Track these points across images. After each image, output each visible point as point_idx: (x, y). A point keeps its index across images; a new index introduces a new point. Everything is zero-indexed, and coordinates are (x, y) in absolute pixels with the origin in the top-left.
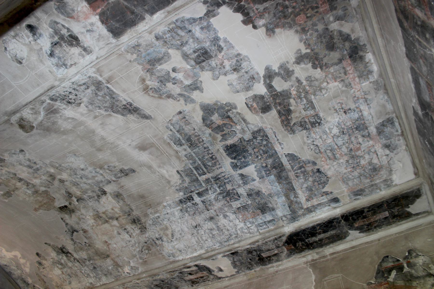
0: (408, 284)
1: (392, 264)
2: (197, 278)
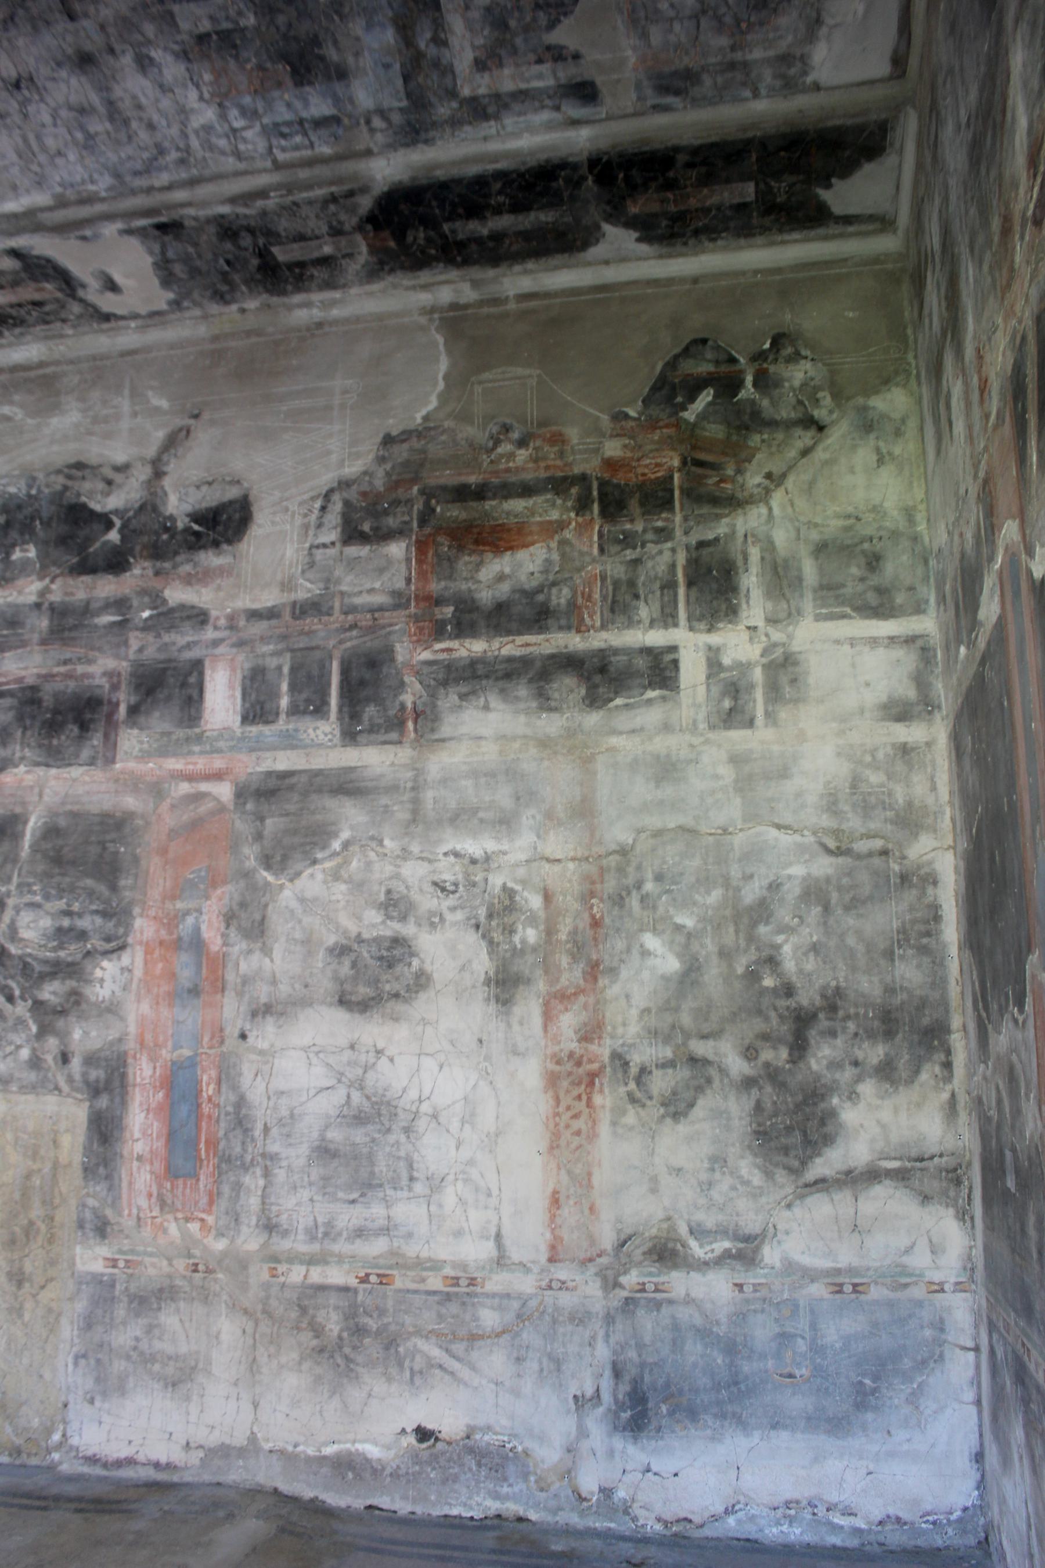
0: (734, 438)
1: (711, 368)
2: (20, 305)
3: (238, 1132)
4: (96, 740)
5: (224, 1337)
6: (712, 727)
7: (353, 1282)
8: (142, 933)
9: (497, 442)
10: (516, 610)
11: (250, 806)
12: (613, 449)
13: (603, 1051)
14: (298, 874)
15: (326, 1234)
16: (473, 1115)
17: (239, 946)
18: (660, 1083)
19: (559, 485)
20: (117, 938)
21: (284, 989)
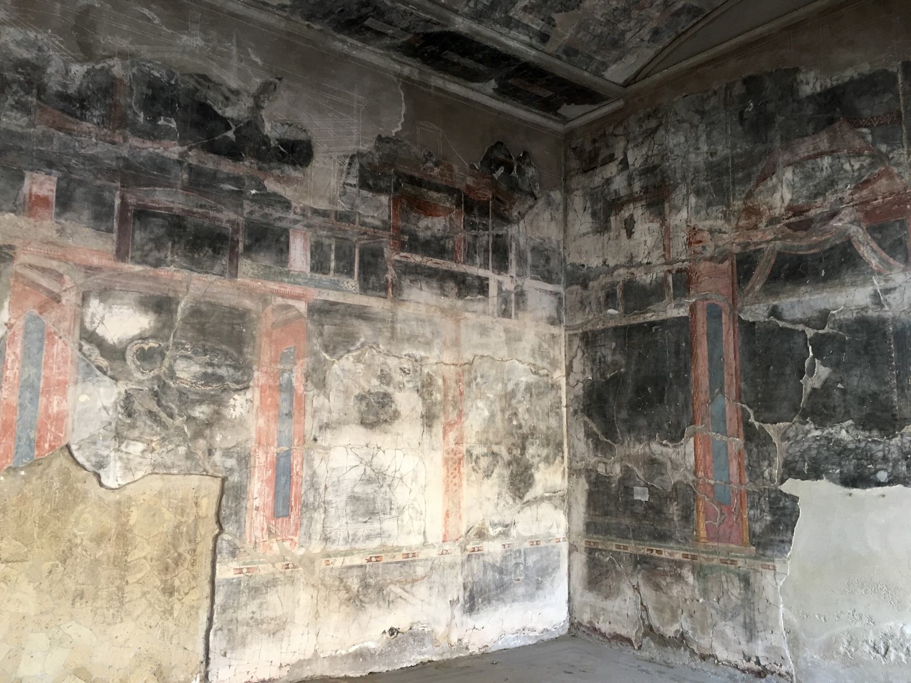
3: (312, 491)
4: (225, 261)
5: (301, 602)
6: (499, 316)
7: (364, 562)
8: (258, 380)
9: (427, 160)
10: (433, 245)
11: (316, 317)
12: (470, 181)
13: (463, 448)
14: (341, 357)
15: (353, 540)
16: (416, 477)
17: (312, 392)
18: (484, 462)
19: (451, 191)
20: (244, 382)
21: (335, 416)
